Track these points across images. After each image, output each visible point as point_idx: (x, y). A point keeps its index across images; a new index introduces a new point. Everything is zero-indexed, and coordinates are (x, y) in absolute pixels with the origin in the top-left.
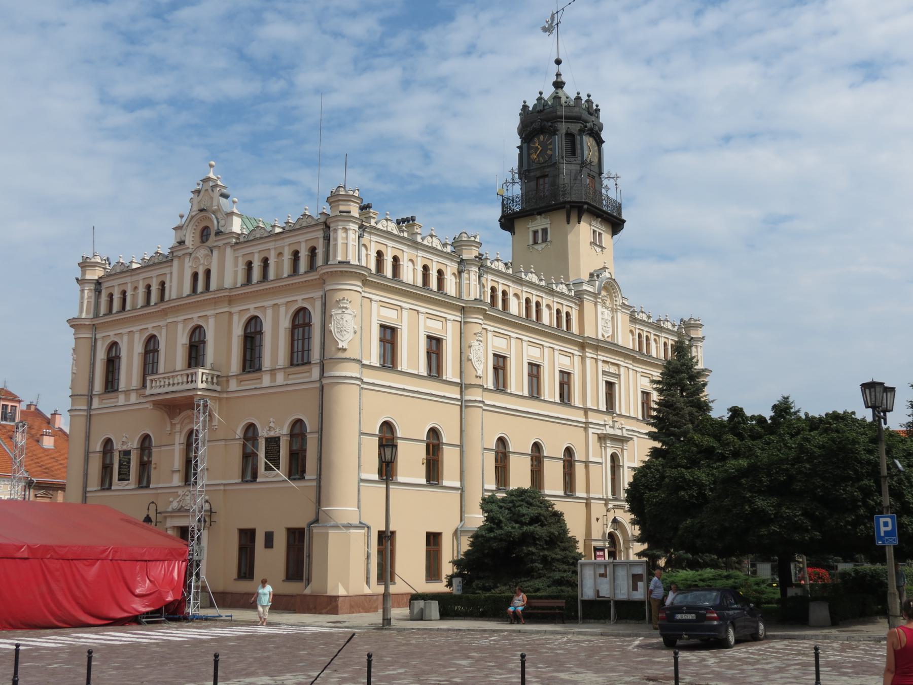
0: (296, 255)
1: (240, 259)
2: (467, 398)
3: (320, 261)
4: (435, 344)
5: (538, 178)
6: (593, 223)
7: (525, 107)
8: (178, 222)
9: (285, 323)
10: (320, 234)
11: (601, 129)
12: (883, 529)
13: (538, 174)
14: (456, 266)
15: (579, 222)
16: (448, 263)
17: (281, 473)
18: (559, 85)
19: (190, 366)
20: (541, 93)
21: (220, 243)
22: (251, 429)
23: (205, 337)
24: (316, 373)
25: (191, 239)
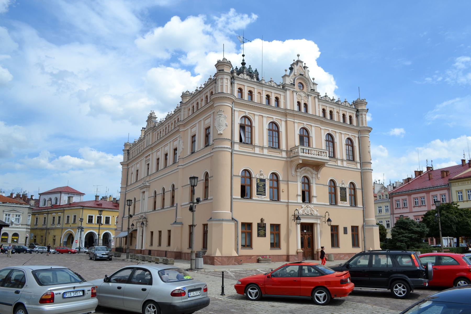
10: (355, 113)
17: (347, 203)
18: (243, 64)
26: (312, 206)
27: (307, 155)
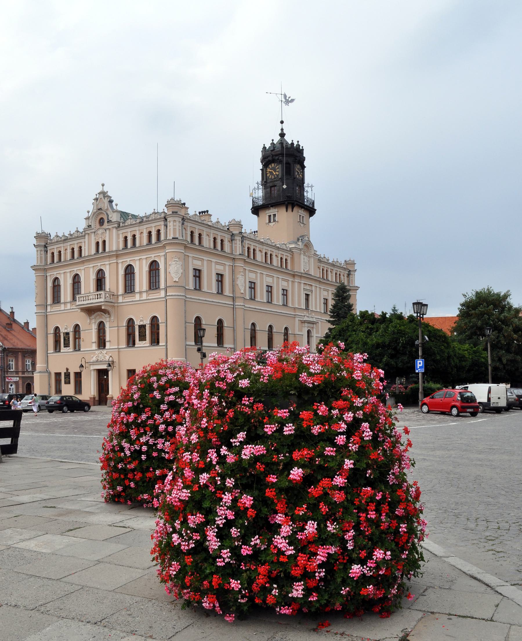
0: (150, 233)
1: (121, 235)
2: (237, 304)
3: (162, 237)
4: (220, 278)
5: (271, 187)
6: (300, 211)
7: (264, 148)
8: (86, 215)
9: (146, 269)
11: (304, 160)
12: (419, 366)
13: (271, 184)
14: (230, 237)
15: (292, 211)
16: (226, 235)
18: (282, 135)
19: (97, 290)
20: (273, 140)
21: (110, 227)
22: (131, 322)
23: (105, 275)
24: (162, 294)
25: (95, 224)
26: (104, 351)
27: (97, 301)
